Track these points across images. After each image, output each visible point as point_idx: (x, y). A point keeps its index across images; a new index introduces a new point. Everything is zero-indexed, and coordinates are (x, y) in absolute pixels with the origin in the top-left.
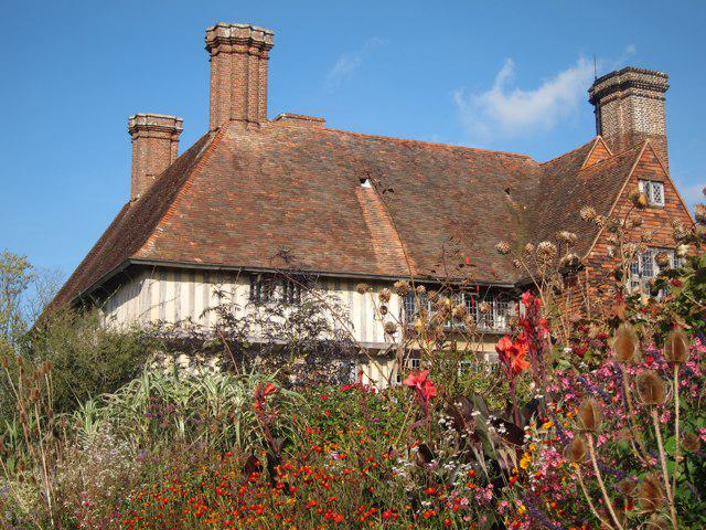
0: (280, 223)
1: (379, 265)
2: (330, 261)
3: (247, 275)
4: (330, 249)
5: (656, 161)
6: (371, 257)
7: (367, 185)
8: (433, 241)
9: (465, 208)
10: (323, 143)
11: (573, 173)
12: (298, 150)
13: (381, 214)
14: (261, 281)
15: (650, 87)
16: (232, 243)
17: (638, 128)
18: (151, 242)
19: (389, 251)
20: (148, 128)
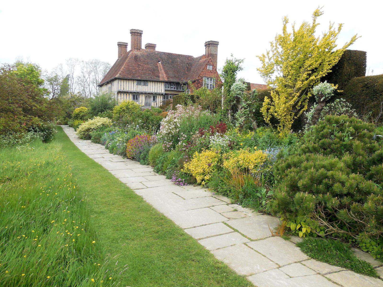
0: (143, 70)
1: (160, 79)
2: (151, 78)
3: (137, 80)
4: (152, 75)
5: (211, 61)
6: (159, 77)
7: (160, 62)
8: (171, 74)
9: (178, 67)
10: (152, 53)
11: (199, 61)
12: (147, 55)
13: (162, 68)
14: (139, 81)
15: (215, 44)
16: (134, 74)
17: (212, 53)
18: (119, 74)
19: (163, 76)
20: (122, 45)
